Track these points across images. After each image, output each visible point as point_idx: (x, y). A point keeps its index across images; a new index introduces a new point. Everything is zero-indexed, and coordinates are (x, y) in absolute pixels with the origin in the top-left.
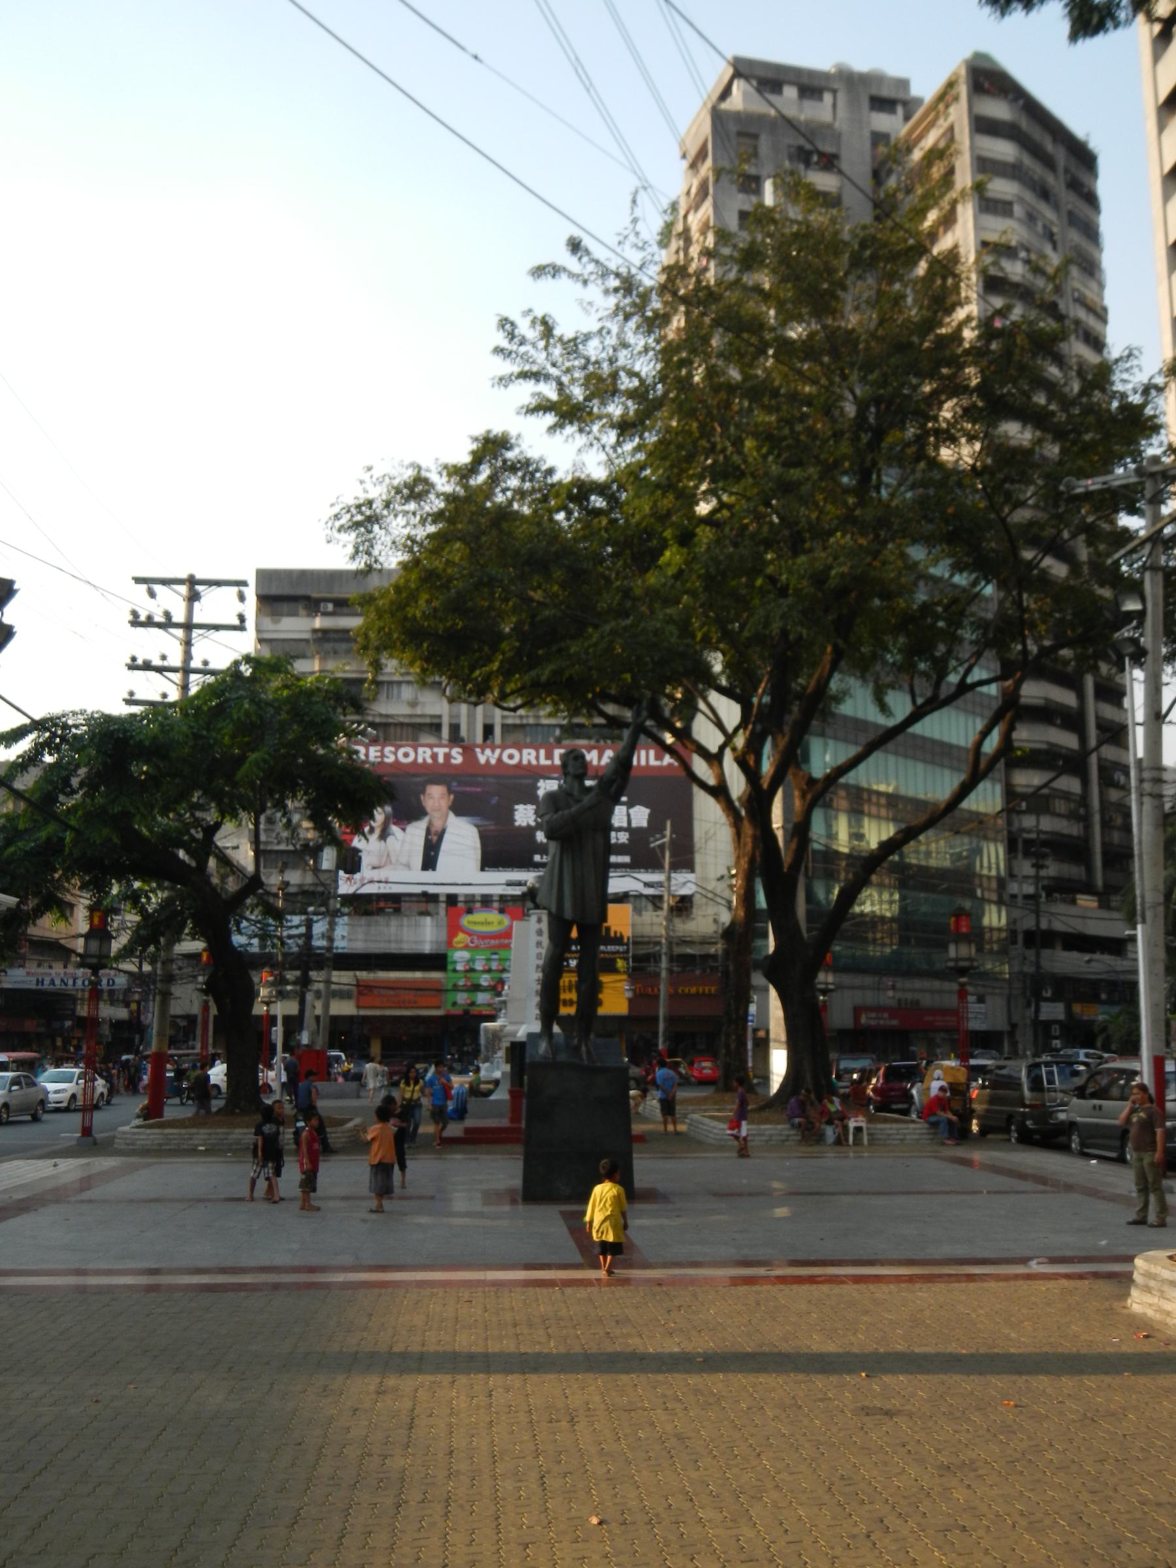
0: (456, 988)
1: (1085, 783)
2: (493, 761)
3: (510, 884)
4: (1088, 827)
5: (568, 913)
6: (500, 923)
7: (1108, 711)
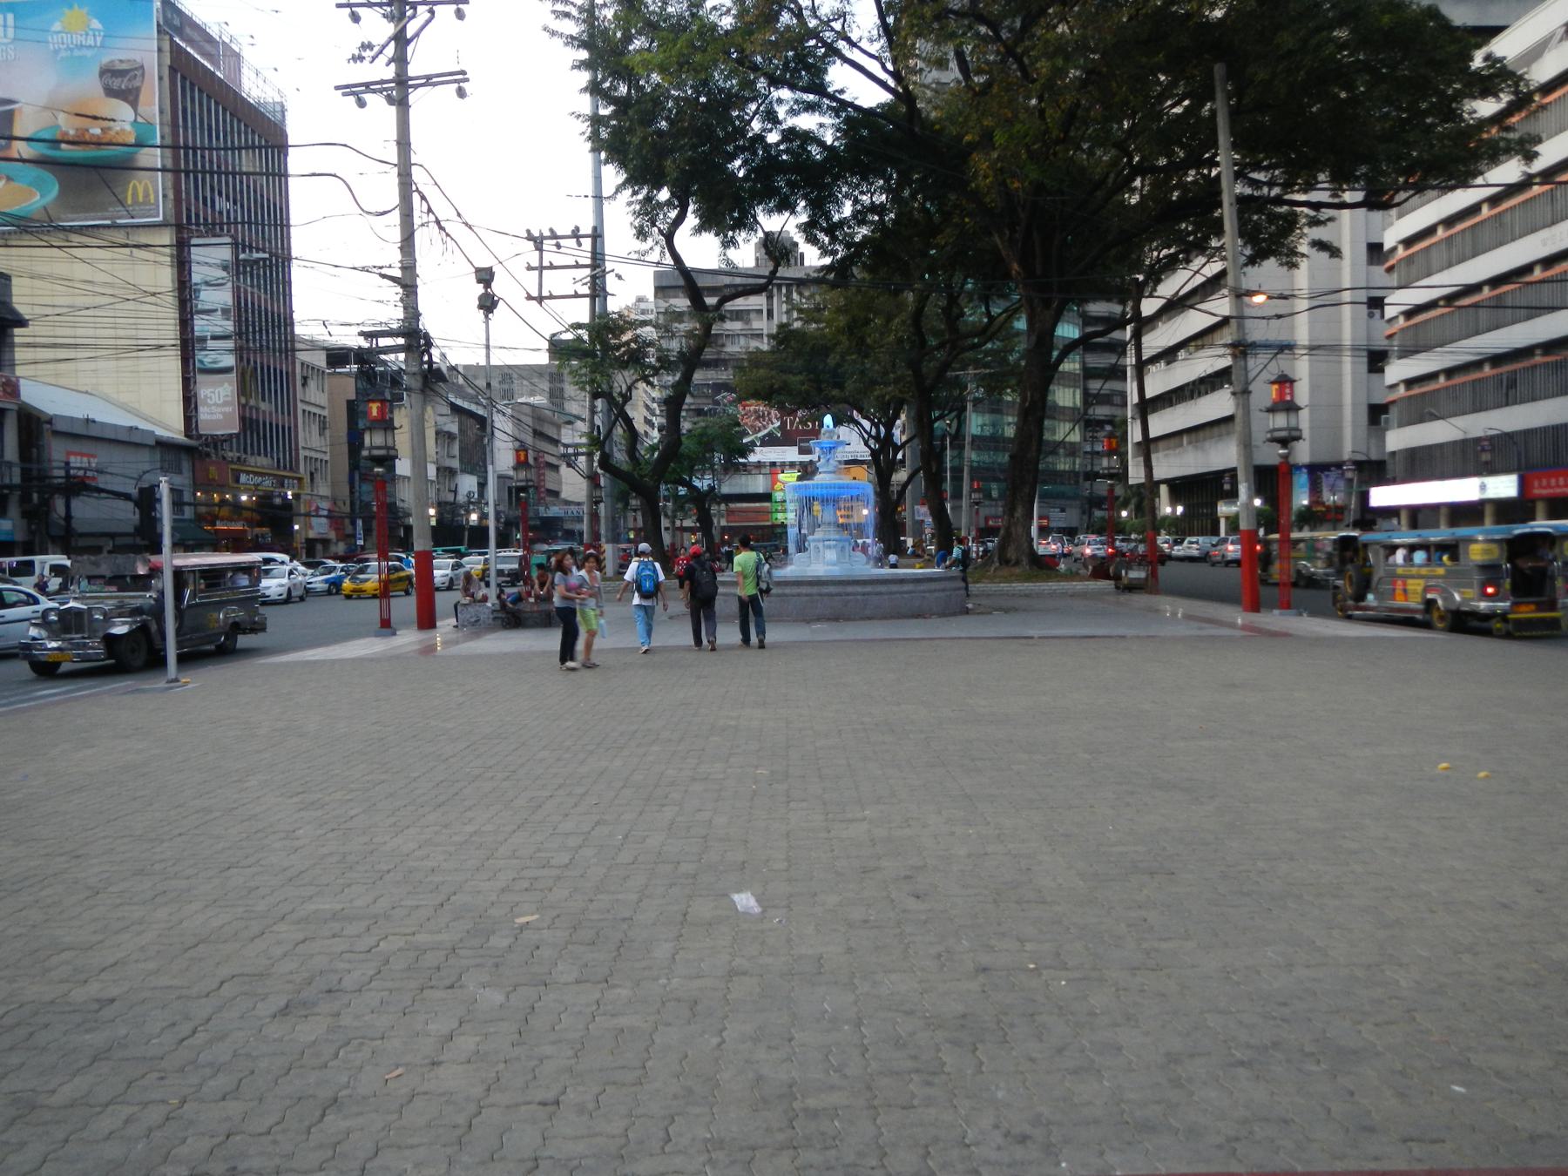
0: (777, 511)
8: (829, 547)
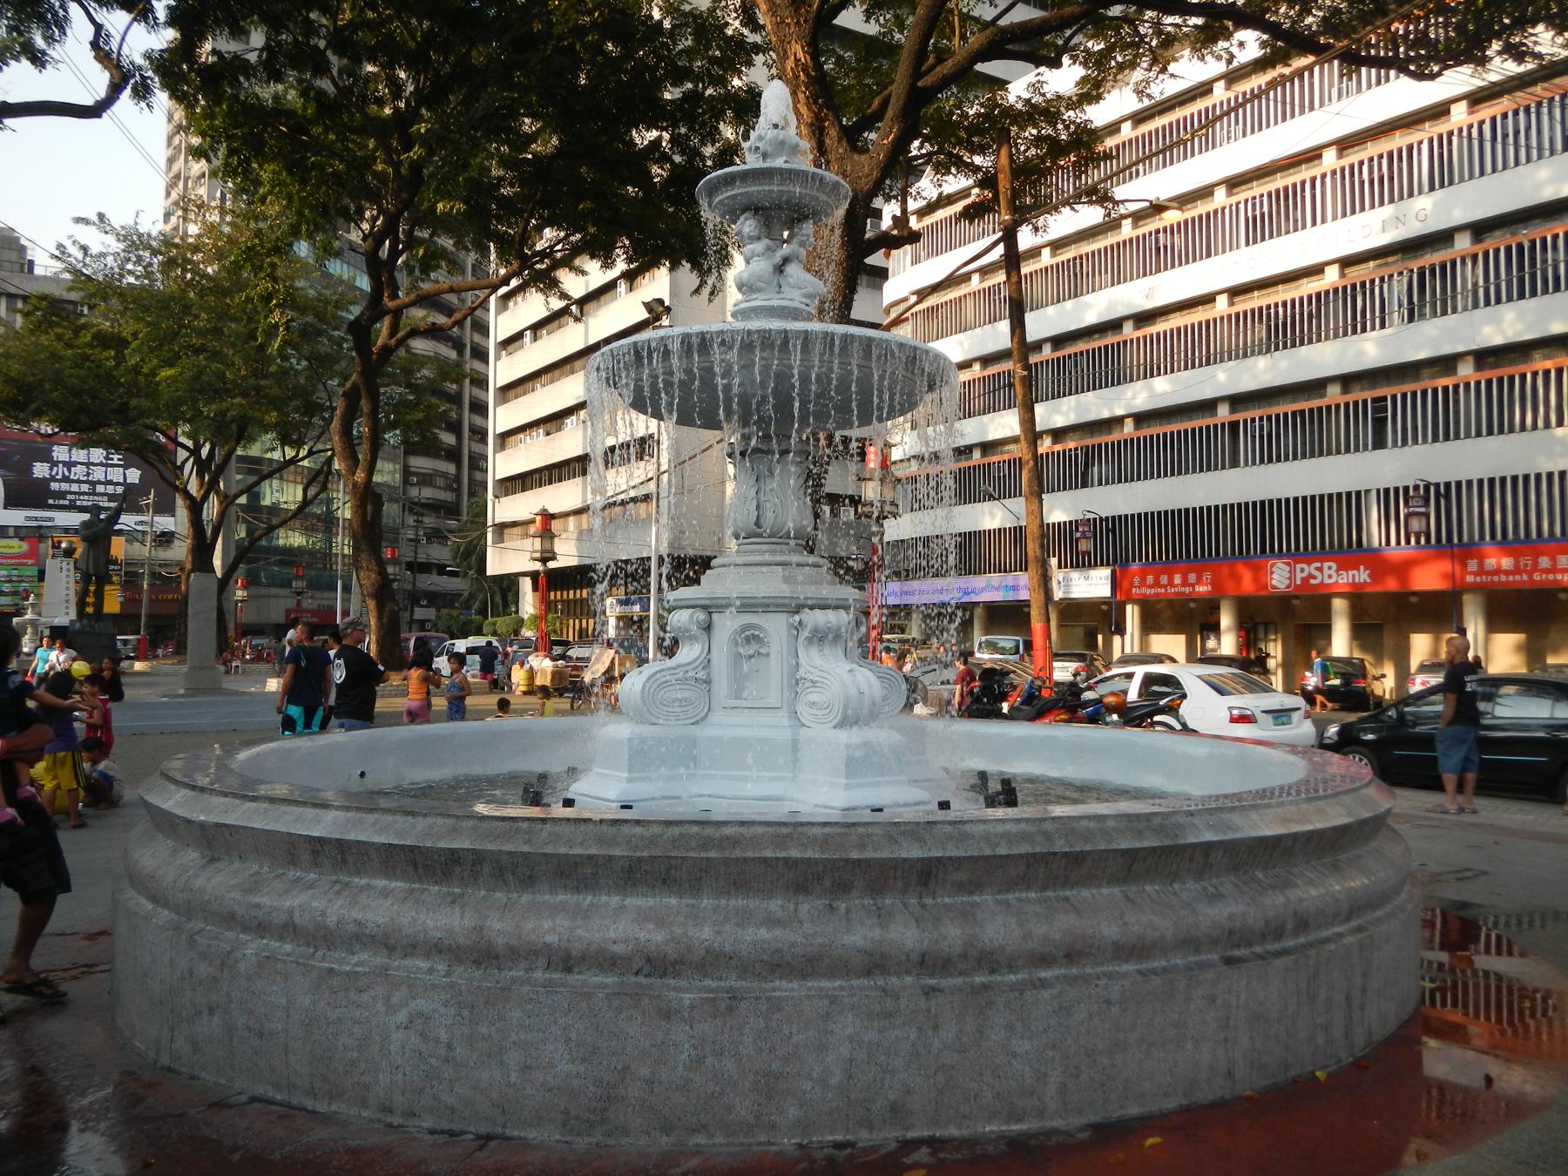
1: (459, 467)
3: (29, 518)
4: (459, 496)
5: (91, 571)
7: (478, 420)
8: (820, 637)
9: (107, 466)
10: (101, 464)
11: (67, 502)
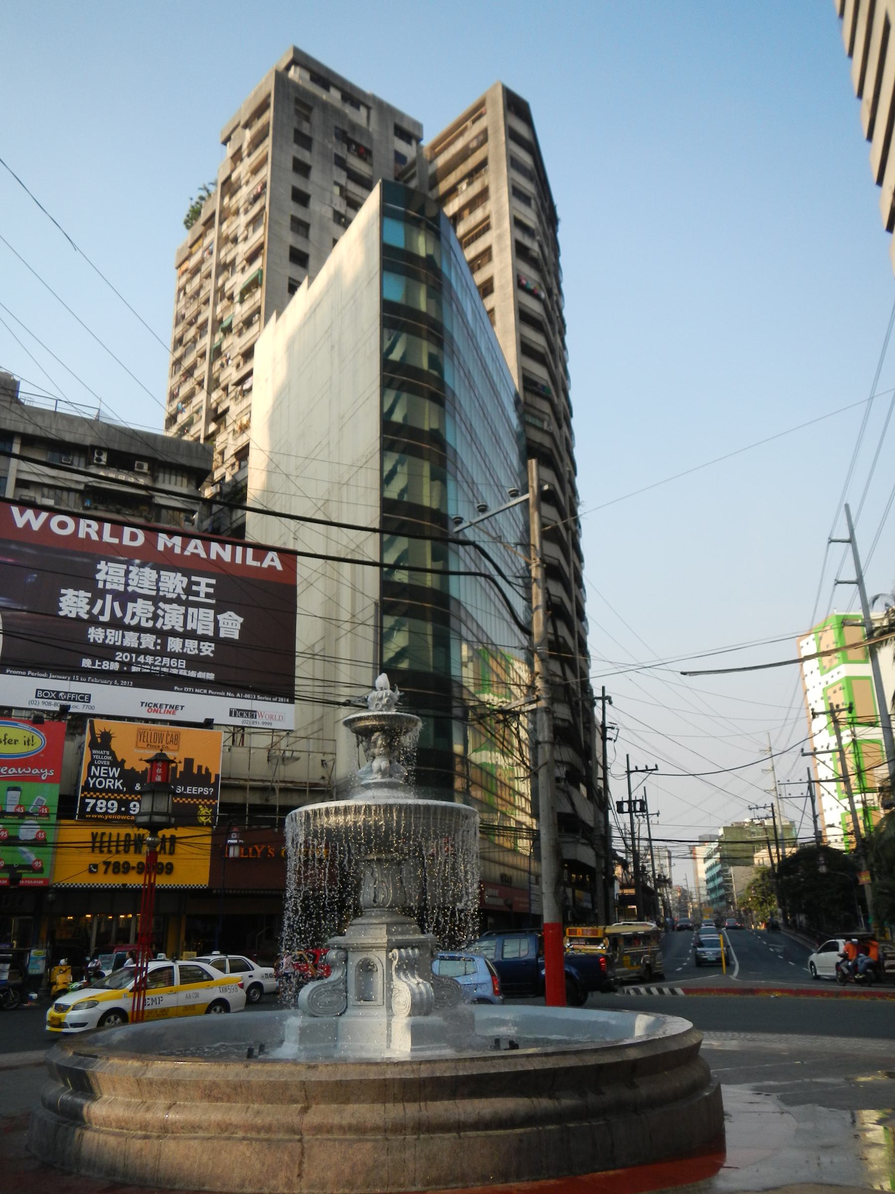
2: (36, 525)
3: (43, 694)
6: (27, 743)
9: (188, 604)
10: (178, 601)
11: (115, 666)
